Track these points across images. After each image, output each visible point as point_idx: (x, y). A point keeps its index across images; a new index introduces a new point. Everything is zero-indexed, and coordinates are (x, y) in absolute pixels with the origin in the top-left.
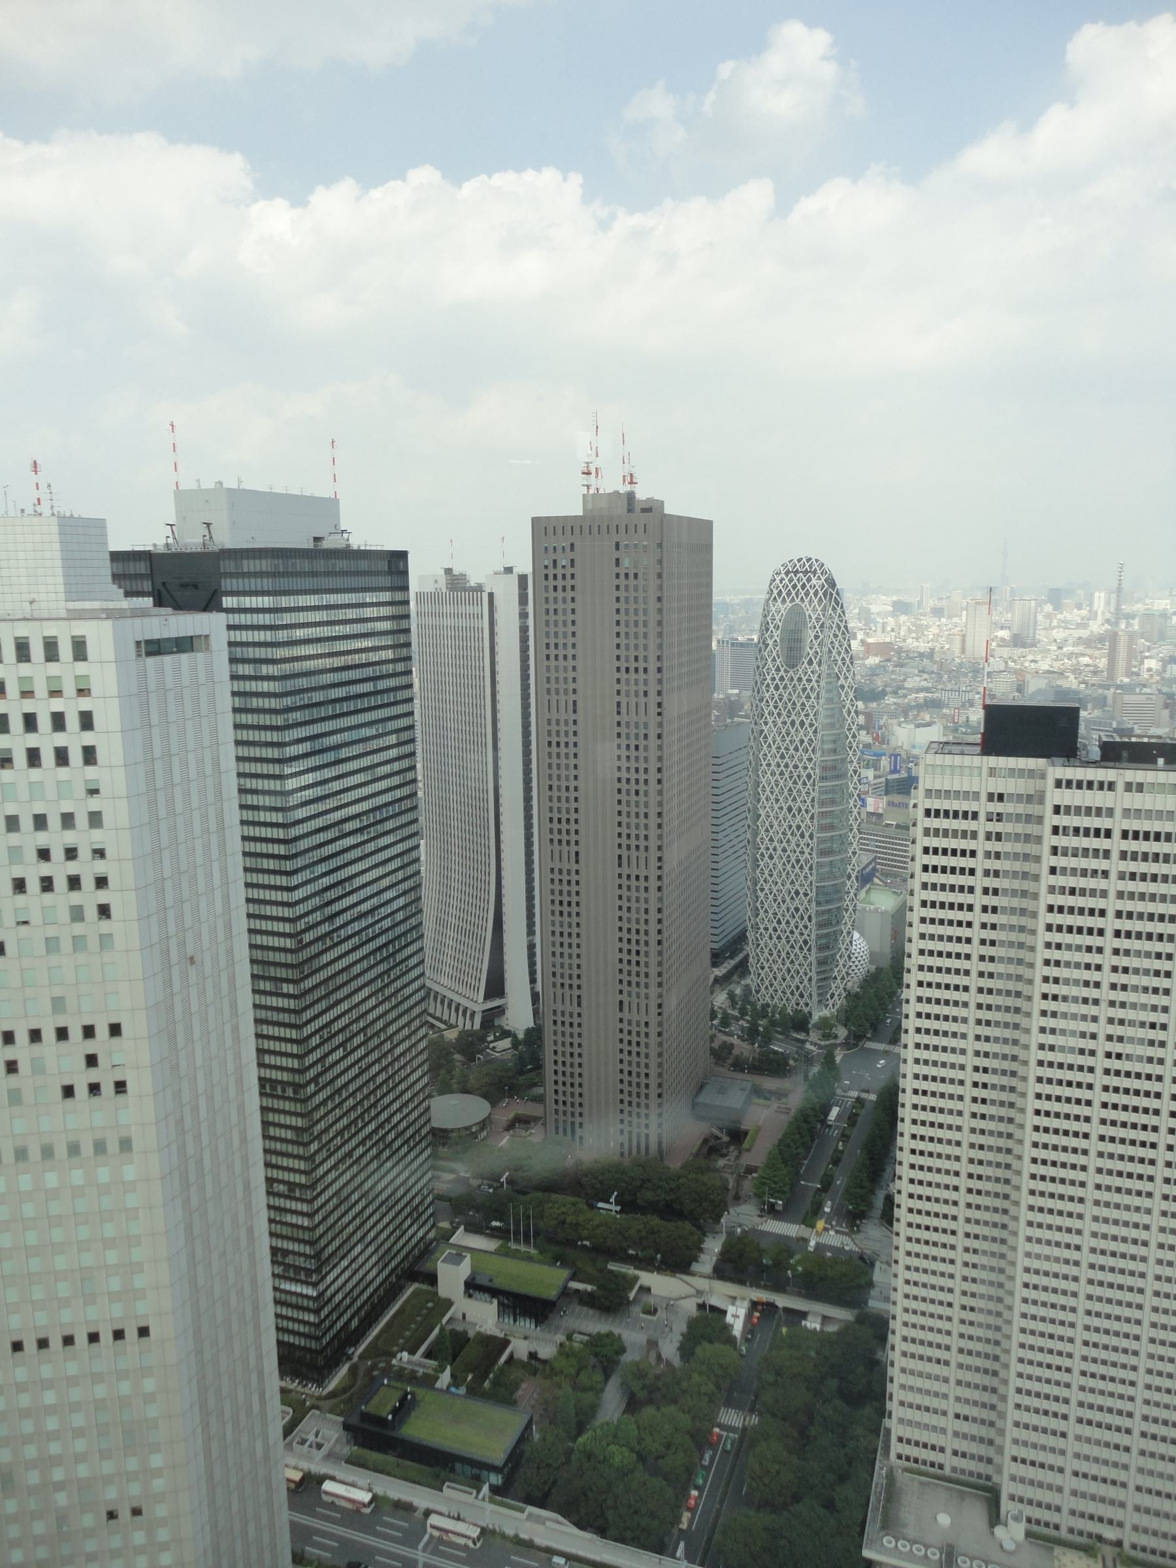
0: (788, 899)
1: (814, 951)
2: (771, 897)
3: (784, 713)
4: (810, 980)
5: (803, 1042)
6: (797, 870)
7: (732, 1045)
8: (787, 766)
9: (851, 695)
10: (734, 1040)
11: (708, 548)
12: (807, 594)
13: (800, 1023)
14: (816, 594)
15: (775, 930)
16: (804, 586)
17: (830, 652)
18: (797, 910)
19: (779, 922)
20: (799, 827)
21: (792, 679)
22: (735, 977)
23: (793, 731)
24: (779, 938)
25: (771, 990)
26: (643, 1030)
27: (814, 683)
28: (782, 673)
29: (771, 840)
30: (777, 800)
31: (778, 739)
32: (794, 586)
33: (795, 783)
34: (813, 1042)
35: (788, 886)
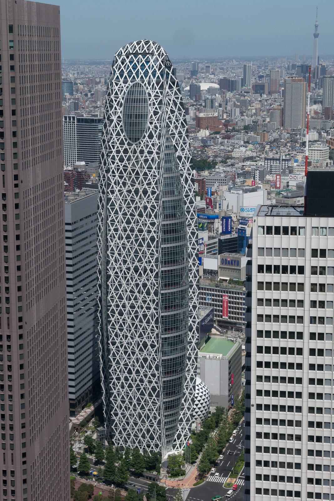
0: (137, 351)
1: (162, 396)
2: (122, 350)
3: (129, 183)
4: (159, 423)
6: (144, 324)
8: (132, 230)
9: (188, 165)
10: (94, 482)
12: (146, 73)
14: (154, 74)
15: (126, 379)
16: (143, 66)
17: (168, 126)
18: (145, 360)
19: (130, 372)
20: (145, 285)
21: (135, 152)
23: (137, 199)
24: (130, 386)
25: (124, 435)
27: (155, 155)
28: (126, 146)
29: (121, 298)
30: (125, 262)
31: (124, 206)
32: (135, 67)
33: (140, 245)
35: (137, 339)
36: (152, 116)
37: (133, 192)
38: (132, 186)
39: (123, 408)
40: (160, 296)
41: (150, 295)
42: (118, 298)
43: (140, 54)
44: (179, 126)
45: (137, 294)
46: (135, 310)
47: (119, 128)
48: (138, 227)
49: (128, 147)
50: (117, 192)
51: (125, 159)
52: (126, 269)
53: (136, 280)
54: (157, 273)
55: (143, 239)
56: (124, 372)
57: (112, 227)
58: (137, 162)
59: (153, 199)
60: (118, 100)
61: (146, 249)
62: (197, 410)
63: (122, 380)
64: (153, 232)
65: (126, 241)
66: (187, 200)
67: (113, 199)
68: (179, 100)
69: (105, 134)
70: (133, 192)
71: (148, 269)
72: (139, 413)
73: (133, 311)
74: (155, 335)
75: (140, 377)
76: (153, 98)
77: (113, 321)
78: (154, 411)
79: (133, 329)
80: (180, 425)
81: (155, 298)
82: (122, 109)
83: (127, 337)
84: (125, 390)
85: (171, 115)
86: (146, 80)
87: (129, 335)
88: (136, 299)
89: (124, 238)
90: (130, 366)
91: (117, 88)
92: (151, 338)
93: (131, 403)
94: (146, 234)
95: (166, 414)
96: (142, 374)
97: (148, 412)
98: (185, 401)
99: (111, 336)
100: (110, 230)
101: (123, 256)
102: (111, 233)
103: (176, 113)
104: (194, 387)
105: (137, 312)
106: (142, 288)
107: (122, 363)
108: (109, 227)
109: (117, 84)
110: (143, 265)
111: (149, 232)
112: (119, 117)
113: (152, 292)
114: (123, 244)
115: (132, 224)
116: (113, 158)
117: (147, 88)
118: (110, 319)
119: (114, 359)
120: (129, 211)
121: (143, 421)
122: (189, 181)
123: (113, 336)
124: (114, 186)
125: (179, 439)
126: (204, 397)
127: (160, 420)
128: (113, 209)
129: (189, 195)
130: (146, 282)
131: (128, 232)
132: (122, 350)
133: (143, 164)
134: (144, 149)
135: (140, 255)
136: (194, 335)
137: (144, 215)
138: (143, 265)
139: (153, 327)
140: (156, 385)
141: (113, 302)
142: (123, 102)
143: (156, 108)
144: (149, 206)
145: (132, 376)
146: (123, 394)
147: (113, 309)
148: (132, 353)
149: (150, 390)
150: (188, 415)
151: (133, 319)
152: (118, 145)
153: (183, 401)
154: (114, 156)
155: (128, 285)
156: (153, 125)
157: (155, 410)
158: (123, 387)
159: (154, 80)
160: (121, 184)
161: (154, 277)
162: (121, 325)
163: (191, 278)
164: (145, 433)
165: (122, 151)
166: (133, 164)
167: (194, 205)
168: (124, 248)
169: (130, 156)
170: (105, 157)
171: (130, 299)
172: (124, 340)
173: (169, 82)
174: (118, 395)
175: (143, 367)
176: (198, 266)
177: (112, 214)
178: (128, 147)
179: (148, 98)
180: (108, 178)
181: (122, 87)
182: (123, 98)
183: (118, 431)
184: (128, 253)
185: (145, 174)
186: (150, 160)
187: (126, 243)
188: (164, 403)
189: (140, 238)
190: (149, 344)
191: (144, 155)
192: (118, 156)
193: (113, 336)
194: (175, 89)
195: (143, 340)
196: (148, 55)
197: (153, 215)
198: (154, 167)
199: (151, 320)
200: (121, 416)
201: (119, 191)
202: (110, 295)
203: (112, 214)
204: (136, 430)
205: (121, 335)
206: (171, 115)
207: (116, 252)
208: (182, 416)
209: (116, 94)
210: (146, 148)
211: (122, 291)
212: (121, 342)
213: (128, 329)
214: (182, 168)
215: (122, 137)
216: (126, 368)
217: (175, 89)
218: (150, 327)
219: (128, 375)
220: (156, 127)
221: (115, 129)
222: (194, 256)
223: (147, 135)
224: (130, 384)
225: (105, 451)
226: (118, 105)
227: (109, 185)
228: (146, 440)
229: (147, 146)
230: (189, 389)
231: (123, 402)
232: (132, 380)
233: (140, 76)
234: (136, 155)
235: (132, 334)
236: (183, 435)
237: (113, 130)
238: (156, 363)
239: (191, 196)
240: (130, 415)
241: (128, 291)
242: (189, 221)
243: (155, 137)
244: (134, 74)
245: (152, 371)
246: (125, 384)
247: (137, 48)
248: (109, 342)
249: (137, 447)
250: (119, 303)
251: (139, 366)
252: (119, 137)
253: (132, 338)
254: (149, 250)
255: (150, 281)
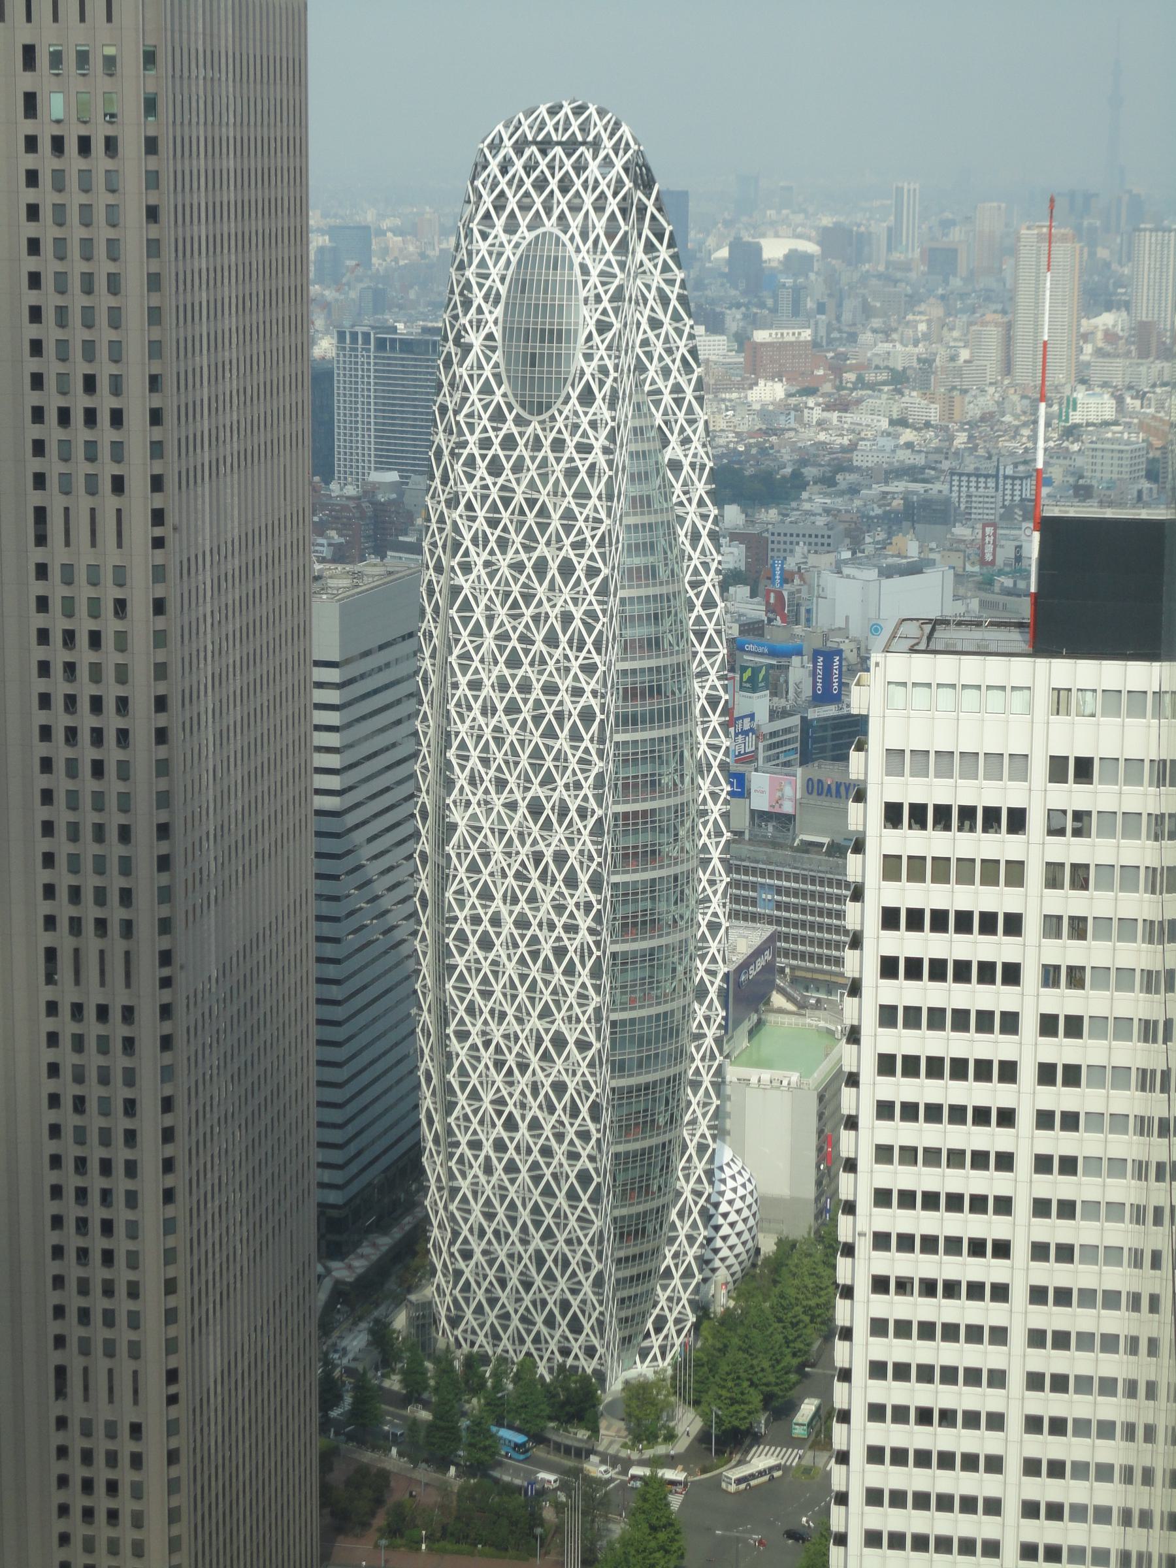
0: (534, 1061)
1: (607, 1202)
2: (487, 1056)
3: (517, 539)
4: (599, 1282)
5: (583, 1453)
6: (558, 977)
7: (384, 1476)
8: (525, 687)
9: (701, 488)
10: (393, 1459)
11: (294, 71)
13: (577, 1401)
15: (500, 1146)
17: (641, 368)
18: (559, 1088)
19: (511, 1125)
20: (561, 858)
21: (537, 444)
22: (391, 1285)
23: (541, 591)
24: (511, 1168)
25: (491, 1316)
26: (126, 1446)
28: (509, 426)
29: (486, 895)
30: (501, 784)
31: (502, 613)
32: (541, 184)
33: (550, 733)
34: (611, 1456)
35: (534, 1023)
36: (589, 337)
37: (529, 570)
38: (528, 549)
39: (490, 1234)
40: (607, 892)
41: (576, 887)
42: (479, 896)
43: (559, 143)
44: (674, 368)
45: (535, 883)
46: (529, 933)
47: (488, 372)
48: (544, 678)
49: (515, 430)
50: (479, 569)
51: (508, 466)
52: (505, 805)
53: (535, 843)
54: (600, 820)
55: (559, 716)
56: (494, 1125)
57: (464, 674)
58: (544, 478)
59: (591, 592)
60: (488, 283)
61: (566, 748)
62: (719, 1243)
63: (488, 1148)
64: (588, 694)
65: (504, 719)
66: (698, 595)
67: (466, 591)
68: (677, 289)
69: (446, 389)
70: (529, 570)
71: (573, 807)
72: (538, 1252)
73: (523, 937)
74: (590, 1010)
75: (541, 1141)
76: (594, 279)
77: (461, 967)
78: (585, 1246)
79: (522, 992)
80: (664, 1288)
81: (593, 898)
82: (499, 311)
83: (503, 1015)
84: (494, 1180)
85: (651, 335)
86: (575, 223)
87: (511, 1011)
88: (532, 898)
89: (500, 712)
90: (510, 1107)
91: (484, 246)
92: (578, 1021)
93: (513, 1221)
94: (567, 699)
95: (621, 1254)
96: (547, 1131)
97: (566, 1249)
98: (681, 1215)
99: (454, 1014)
100: (455, 686)
101: (494, 766)
102: (459, 693)
103: (668, 327)
104: (710, 1174)
105: (535, 940)
106: (552, 866)
107: (487, 1097)
108: (454, 674)
109: (485, 236)
110: (556, 795)
111: (577, 692)
112: (490, 337)
113: (584, 878)
114: (497, 729)
115: (526, 667)
116: (471, 462)
117: (578, 250)
118: (452, 961)
119: (463, 1085)
120: (515, 629)
121: (550, 1276)
122: (705, 540)
123: (461, 1012)
124: (472, 549)
125: (658, 1330)
126: (738, 1204)
127: (600, 1275)
128: (465, 621)
129: (703, 582)
130: (566, 847)
131: (513, 692)
132: (487, 1056)
133: (563, 483)
134: (566, 435)
135: (549, 763)
136: (712, 1014)
137: (563, 640)
138: (556, 795)
139: (583, 986)
140: (590, 1166)
141: (462, 908)
142: (503, 291)
143: (605, 312)
144: (578, 613)
145: (518, 1136)
146: (488, 1191)
147: (461, 931)
148: (519, 1065)
149: (572, 1179)
150: (690, 1258)
151: (522, 961)
152: (485, 422)
153: (673, 1216)
154: (472, 457)
155: (509, 854)
156: (595, 363)
157: (585, 1242)
158: (488, 1169)
159: (600, 225)
160: (492, 544)
161: (591, 834)
162: (485, 981)
163: (704, 839)
164: (556, 1312)
165: (497, 442)
166: (532, 485)
167: (717, 611)
168: (499, 742)
169: (521, 458)
170: (446, 458)
171: (515, 900)
172: (493, 1026)
173: (646, 231)
174: (475, 1193)
175: (552, 1110)
176: (726, 802)
177: (465, 636)
178: (515, 430)
179: (580, 278)
180: (455, 523)
181: (502, 245)
182: (503, 279)
183: (473, 1306)
184: (511, 758)
185: (568, 515)
186: (583, 470)
187: (506, 725)
188: (615, 1220)
189: (550, 711)
190: (571, 1040)
191: (566, 455)
192: (483, 457)
193: (461, 1012)
194: (664, 253)
195: (554, 1028)
196: (582, 149)
197: (589, 641)
198: (594, 493)
199: (579, 967)
200: (482, 1260)
201: (487, 564)
202: (454, 887)
203: (465, 636)
204: (527, 1301)
205: (486, 1010)
206: (651, 335)
207: (475, 754)
208: (669, 1261)
209: (483, 264)
210: (572, 434)
211: (492, 874)
212: (484, 1033)
213: (509, 991)
214: (684, 498)
215: (498, 397)
216: (499, 1113)
217: (664, 253)
218: (576, 988)
219: (505, 1135)
220: (603, 370)
221: (475, 372)
222: (715, 769)
223: (574, 395)
224: (511, 1161)
225: (429, 1365)
226: (486, 298)
227: (457, 545)
228: (558, 1334)
229: (576, 426)
230: (693, 1179)
231: (490, 1217)
232: (518, 1149)
233: (556, 213)
234: (541, 455)
235: (519, 1009)
236: (671, 1319)
237: (471, 377)
238: (592, 1097)
239: (708, 585)
240: (510, 1256)
241: (510, 874)
242: (701, 662)
243: (599, 401)
244: (538, 205)
245: (578, 1121)
246: (495, 1162)
247: (550, 127)
248: (450, 1031)
249: (529, 1354)
250: (480, 911)
251: (540, 1107)
252: (488, 398)
253: (520, 1021)
254: (576, 748)
255: (578, 846)
